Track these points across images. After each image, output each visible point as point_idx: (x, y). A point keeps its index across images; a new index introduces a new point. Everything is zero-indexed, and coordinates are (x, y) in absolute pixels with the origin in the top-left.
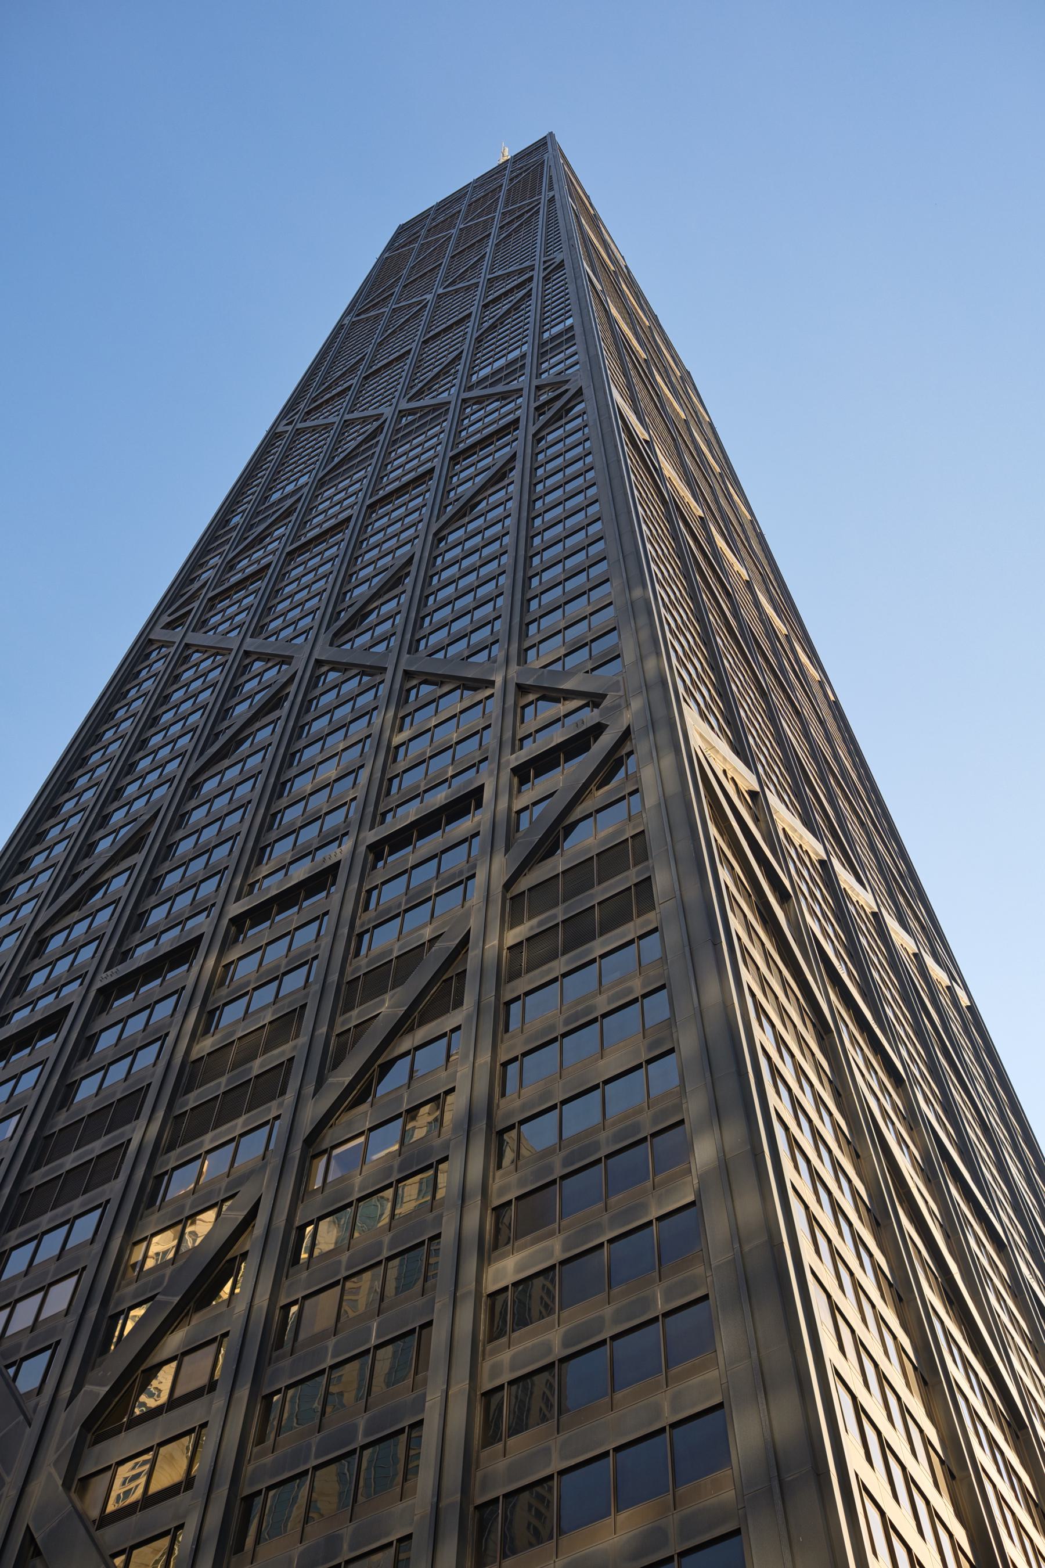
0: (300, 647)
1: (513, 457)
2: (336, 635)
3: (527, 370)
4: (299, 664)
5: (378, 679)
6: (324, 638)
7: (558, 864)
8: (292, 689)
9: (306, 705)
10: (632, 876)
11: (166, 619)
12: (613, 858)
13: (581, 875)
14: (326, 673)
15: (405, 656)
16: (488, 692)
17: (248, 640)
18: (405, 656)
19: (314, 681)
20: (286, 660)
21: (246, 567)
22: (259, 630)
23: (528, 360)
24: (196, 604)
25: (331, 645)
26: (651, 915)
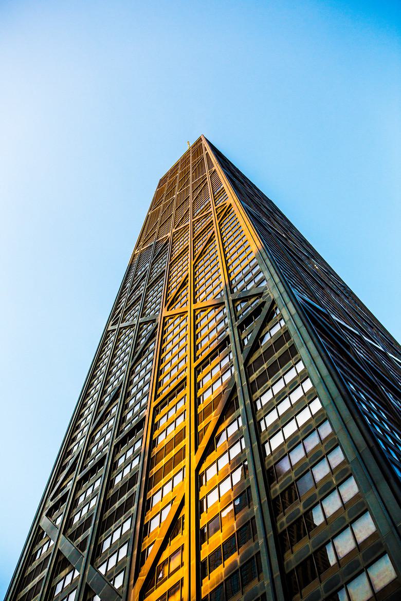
0: (158, 315)
1: (214, 233)
3: (212, 206)
5: (185, 316)
6: (165, 309)
8: (158, 329)
9: (164, 332)
10: (287, 345)
11: (111, 323)
13: (269, 352)
16: (223, 306)
17: (140, 319)
19: (165, 324)
20: (154, 321)
21: (134, 298)
22: (143, 315)
23: (211, 203)
25: (168, 310)
26: (297, 356)
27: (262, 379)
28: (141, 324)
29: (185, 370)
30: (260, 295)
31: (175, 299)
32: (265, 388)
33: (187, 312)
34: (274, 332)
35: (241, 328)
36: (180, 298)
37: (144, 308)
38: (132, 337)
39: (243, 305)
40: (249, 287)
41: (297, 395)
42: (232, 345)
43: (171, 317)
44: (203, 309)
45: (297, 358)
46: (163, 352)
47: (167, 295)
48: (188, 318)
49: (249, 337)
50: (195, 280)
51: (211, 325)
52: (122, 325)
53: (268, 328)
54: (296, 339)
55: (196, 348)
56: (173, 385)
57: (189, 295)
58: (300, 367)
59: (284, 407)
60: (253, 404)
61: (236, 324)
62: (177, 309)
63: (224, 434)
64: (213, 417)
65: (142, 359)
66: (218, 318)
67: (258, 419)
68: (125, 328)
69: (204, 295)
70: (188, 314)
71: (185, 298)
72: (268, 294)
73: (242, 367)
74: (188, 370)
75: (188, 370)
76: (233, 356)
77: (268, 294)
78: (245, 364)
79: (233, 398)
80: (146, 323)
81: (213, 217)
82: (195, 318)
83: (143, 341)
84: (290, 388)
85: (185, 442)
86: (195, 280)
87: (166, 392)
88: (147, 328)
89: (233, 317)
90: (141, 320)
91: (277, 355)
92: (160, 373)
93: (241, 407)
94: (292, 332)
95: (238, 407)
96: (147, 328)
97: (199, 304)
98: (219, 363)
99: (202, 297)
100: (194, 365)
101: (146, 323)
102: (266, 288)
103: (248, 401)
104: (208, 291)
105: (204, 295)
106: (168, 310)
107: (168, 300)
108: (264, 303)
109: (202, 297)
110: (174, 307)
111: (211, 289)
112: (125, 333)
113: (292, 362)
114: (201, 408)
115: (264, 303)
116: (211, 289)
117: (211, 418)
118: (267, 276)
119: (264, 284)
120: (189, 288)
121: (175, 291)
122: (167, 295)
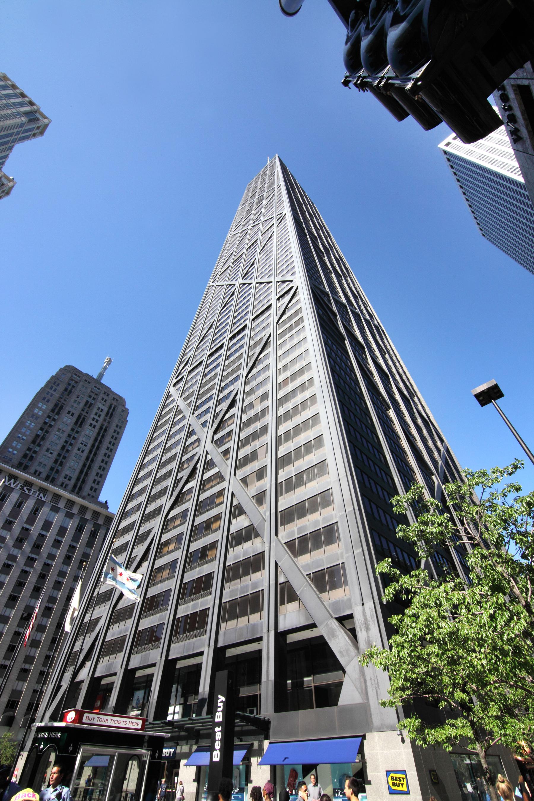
2: (243, 278)
4: (236, 286)
6: (241, 279)
10: (300, 316)
12: (296, 313)
13: (290, 318)
27: (284, 332)
30: (291, 281)
54: (304, 314)
64: (258, 349)
78: (277, 323)
81: (275, 221)
85: (242, 361)
108: (292, 288)
115: (292, 288)
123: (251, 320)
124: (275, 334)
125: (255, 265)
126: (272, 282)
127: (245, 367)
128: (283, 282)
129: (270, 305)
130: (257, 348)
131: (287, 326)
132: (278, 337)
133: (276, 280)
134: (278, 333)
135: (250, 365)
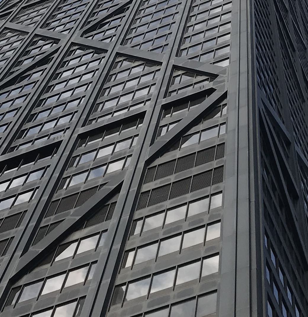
0: (65, 35)
2: (85, 32)
4: (62, 44)
5: (102, 55)
6: (79, 32)
7: (176, 154)
8: (56, 55)
9: (62, 64)
10: (214, 164)
13: (188, 160)
14: (76, 50)
15: (118, 46)
16: (158, 68)
17: (38, 29)
18: (118, 46)
19: (69, 53)
20: (56, 41)
22: (46, 25)
24: (14, 9)
25: (82, 36)
27: (161, 194)
28: (36, 35)
29: (64, 130)
30: (212, 77)
31: (100, 24)
32: (157, 208)
33: (106, 51)
34: (207, 136)
35: (167, 108)
36: (106, 27)
37: (52, 16)
38: (15, 49)
39: (185, 78)
40: (204, 58)
41: (194, 239)
42: (142, 126)
43: (82, 47)
44: (131, 58)
45: (218, 188)
46: (47, 92)
47: (92, 14)
48: (103, 61)
49: (171, 127)
50: (138, 11)
51: (129, 85)
52: (9, 25)
53: (200, 127)
54: (228, 161)
55: (94, 107)
56: (40, 144)
57: (120, 29)
58: (217, 201)
59: (171, 246)
60: (132, 223)
61: (164, 101)
62: (95, 40)
63: (74, 246)
64: (72, 216)
65: (13, 87)
66: (144, 80)
67: (127, 248)
68: (12, 30)
69: (140, 40)
70: (107, 55)
71: (113, 31)
72: (224, 81)
73: (141, 165)
74: (68, 132)
75: (68, 132)
76: (138, 144)
77: (224, 81)
78: (148, 162)
79: (110, 202)
80: (44, 38)
82: (114, 65)
83: (28, 63)
84: (190, 225)
85: (16, 233)
86: (138, 11)
87: (24, 149)
88: (41, 47)
89: (164, 89)
90: (39, 31)
91: (195, 170)
92: (30, 117)
93: (114, 221)
94: (229, 149)
95: (109, 218)
96: (41, 47)
97: (127, 49)
98: (115, 144)
99: (136, 41)
100: (81, 130)
101: (44, 38)
102: (224, 71)
103: (126, 217)
104: (149, 36)
105: (140, 40)
106: (82, 36)
107: (89, 22)
108: (211, 91)
109: (136, 41)
110: (93, 36)
111: (153, 35)
112: (9, 38)
113: (209, 190)
114: (61, 194)
115: (211, 91)
116: (153, 35)
117: (67, 215)
118: (235, 57)
119: (226, 63)
120: (125, 19)
121: (105, 13)
122: (92, 14)
123: (75, 136)
124: (134, 188)
125: (127, 13)
126: (160, 64)
127: (19, 253)
128: (190, 72)
129: (141, 116)
130: (72, 211)
131: (172, 178)
132: (140, 200)
133: (173, 62)
134: (145, 188)
135: (37, 249)
